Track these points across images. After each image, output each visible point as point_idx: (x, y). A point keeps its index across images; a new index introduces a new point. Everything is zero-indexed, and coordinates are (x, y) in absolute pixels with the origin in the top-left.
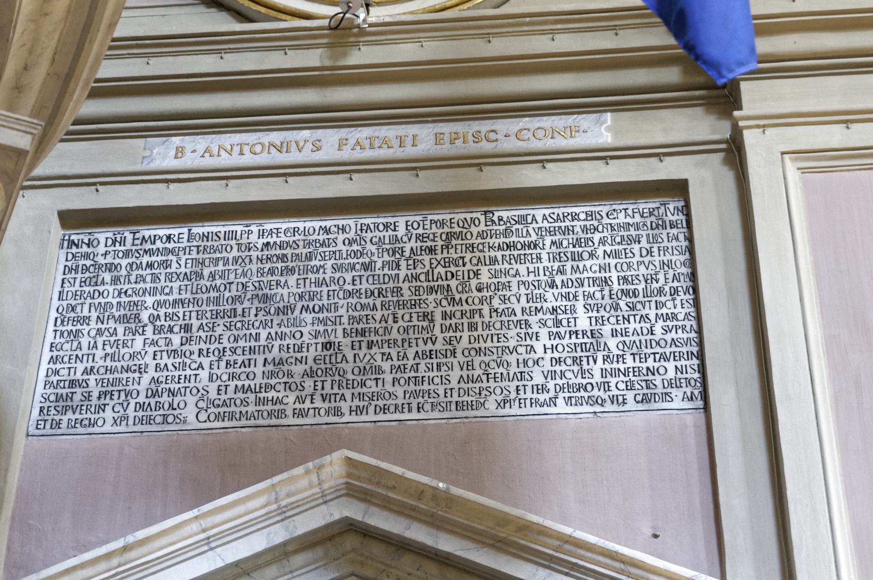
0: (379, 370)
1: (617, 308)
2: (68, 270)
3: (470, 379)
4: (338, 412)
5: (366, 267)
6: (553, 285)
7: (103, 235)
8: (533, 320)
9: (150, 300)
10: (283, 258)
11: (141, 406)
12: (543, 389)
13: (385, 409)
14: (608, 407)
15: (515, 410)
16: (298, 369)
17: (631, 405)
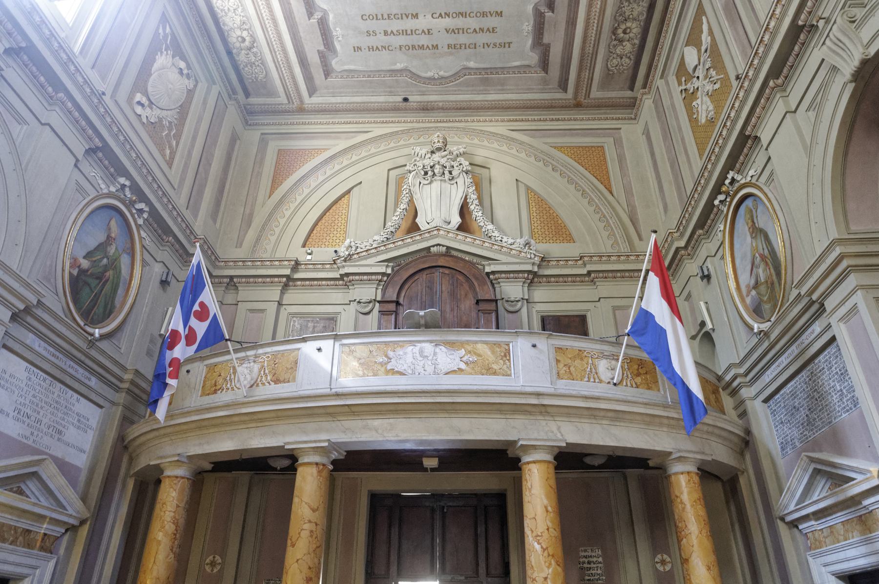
0: (815, 419)
1: (841, 380)
2: (771, 414)
3: (828, 414)
4: (814, 434)
5: (804, 390)
6: (830, 379)
7: (771, 402)
8: (831, 391)
9: (782, 416)
10: (793, 394)
11: (791, 445)
12: (839, 411)
13: (820, 430)
14: (851, 411)
15: (837, 420)
16: (805, 424)
17: (854, 409)
